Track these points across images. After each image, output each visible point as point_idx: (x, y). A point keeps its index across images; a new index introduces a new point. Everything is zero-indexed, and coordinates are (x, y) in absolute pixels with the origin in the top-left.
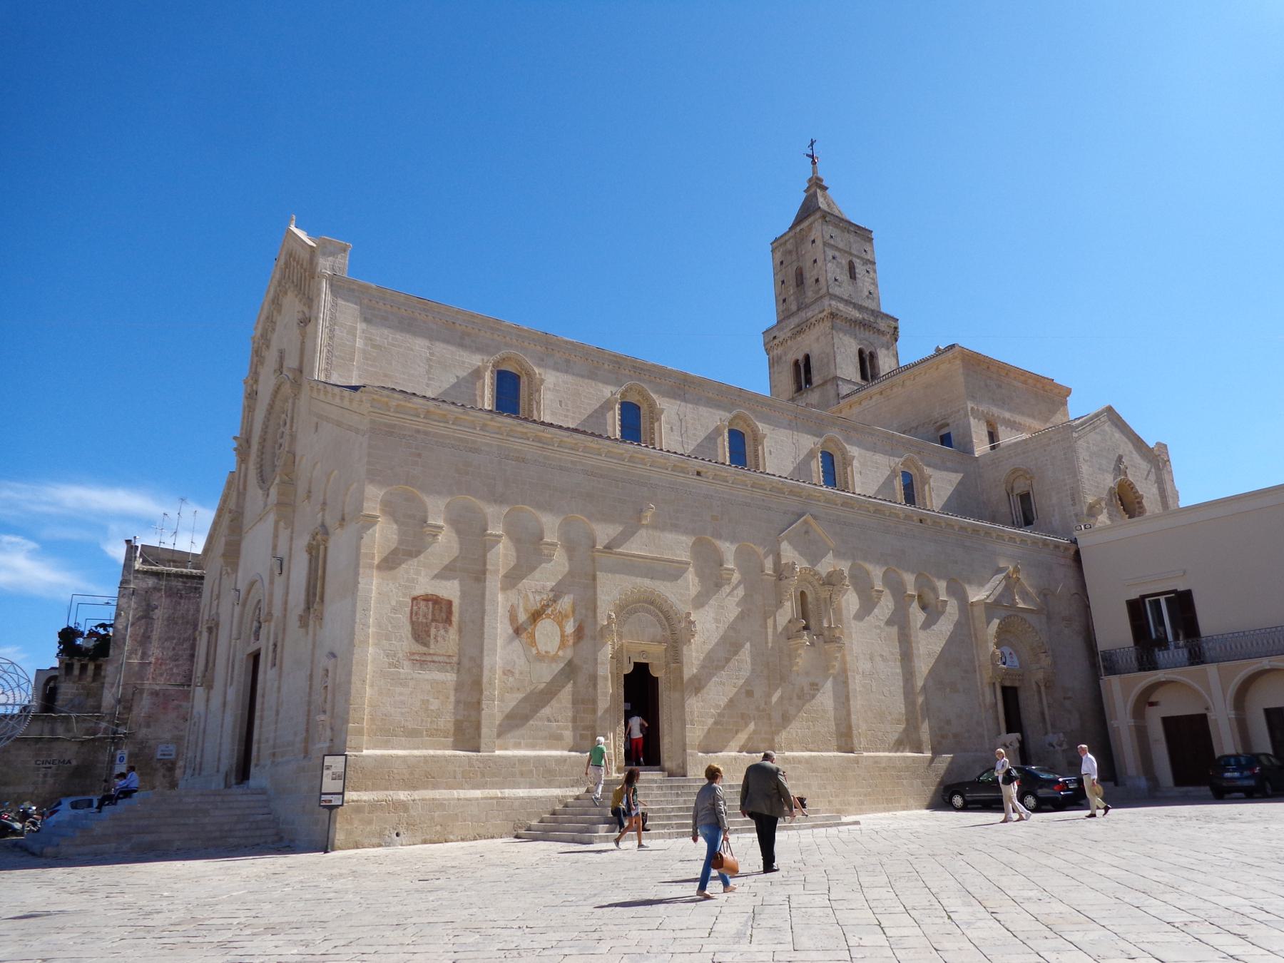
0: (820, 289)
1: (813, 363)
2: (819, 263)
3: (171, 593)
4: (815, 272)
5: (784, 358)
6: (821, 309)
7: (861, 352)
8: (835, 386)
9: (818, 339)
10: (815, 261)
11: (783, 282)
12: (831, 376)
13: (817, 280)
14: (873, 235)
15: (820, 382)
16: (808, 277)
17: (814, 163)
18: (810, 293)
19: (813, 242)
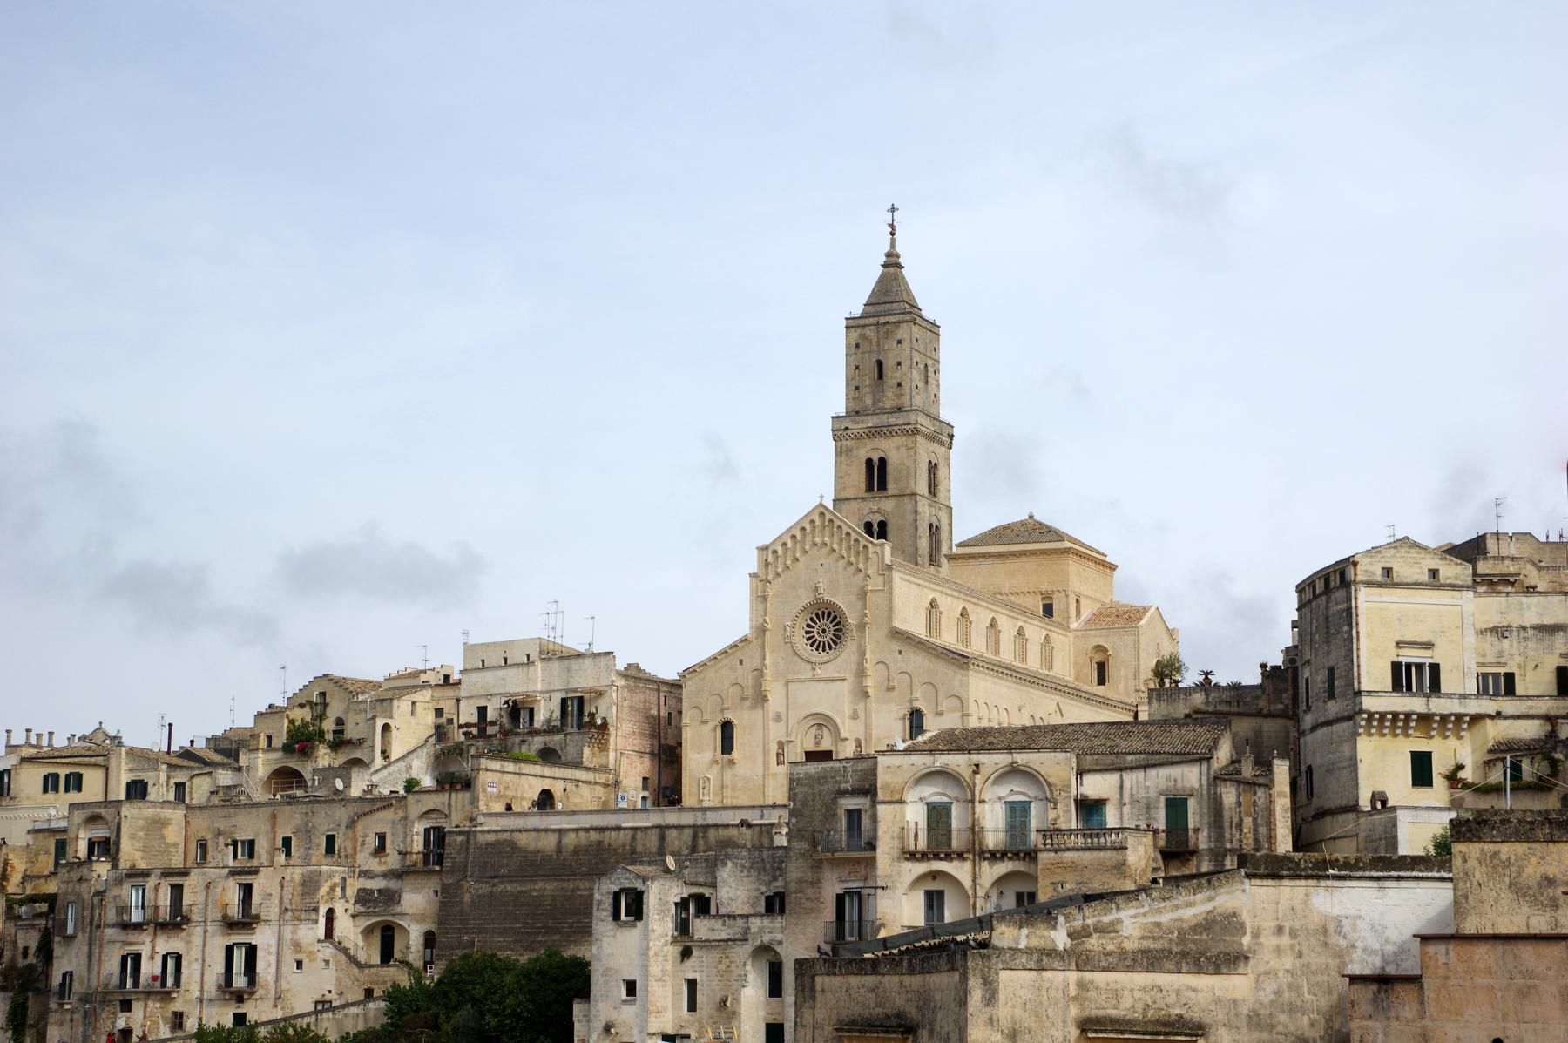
0: (902, 395)
1: (890, 469)
2: (905, 367)
3: (630, 690)
4: (898, 374)
5: (855, 452)
6: (907, 421)
7: (930, 462)
8: (913, 502)
9: (898, 448)
10: (899, 364)
11: (857, 368)
12: (908, 491)
13: (899, 385)
14: (941, 331)
15: (896, 492)
16: (889, 375)
17: (892, 234)
18: (890, 394)
19: (899, 342)
